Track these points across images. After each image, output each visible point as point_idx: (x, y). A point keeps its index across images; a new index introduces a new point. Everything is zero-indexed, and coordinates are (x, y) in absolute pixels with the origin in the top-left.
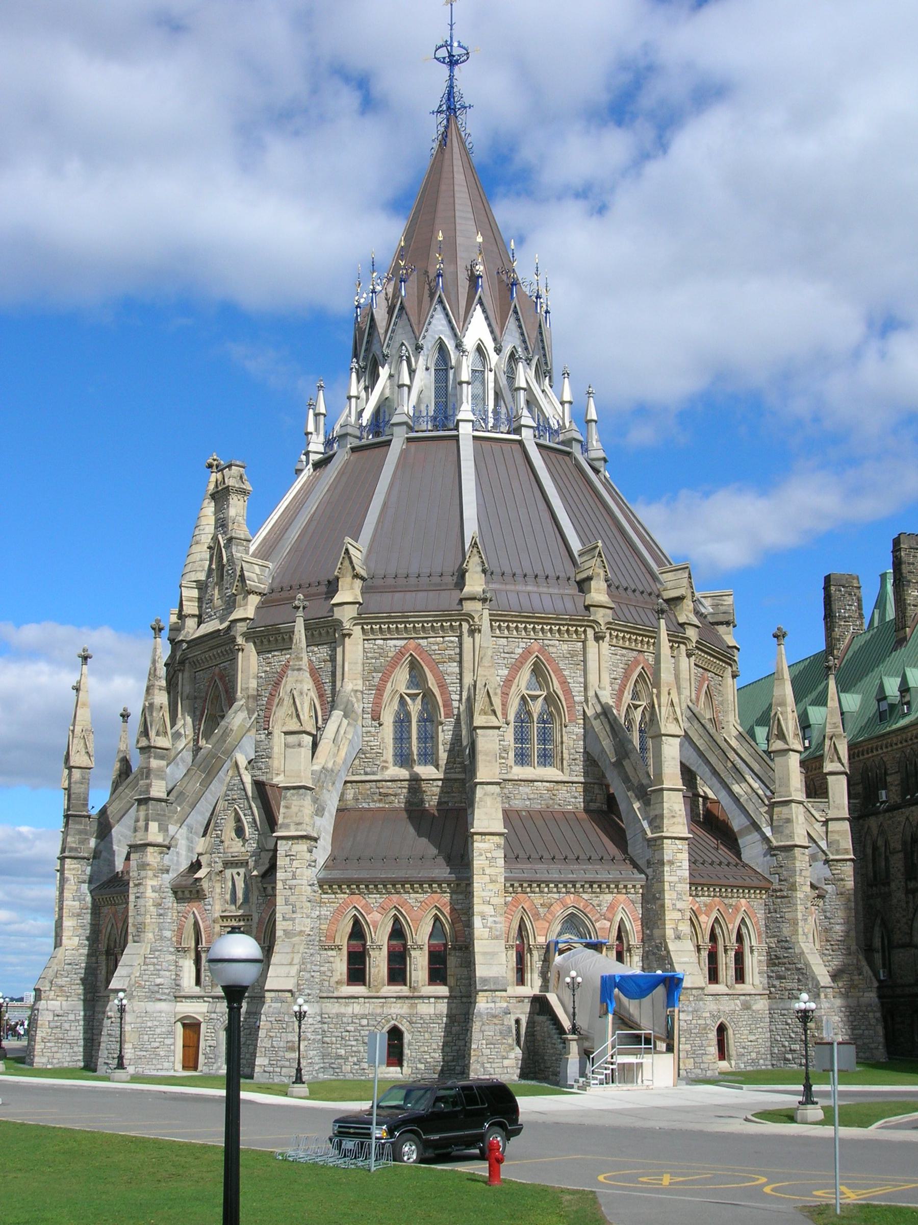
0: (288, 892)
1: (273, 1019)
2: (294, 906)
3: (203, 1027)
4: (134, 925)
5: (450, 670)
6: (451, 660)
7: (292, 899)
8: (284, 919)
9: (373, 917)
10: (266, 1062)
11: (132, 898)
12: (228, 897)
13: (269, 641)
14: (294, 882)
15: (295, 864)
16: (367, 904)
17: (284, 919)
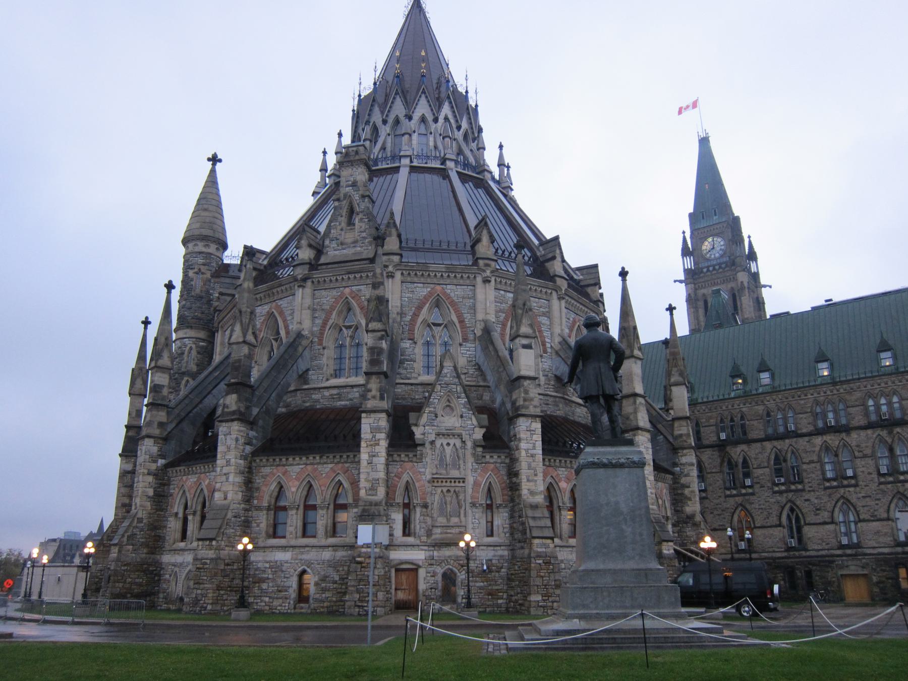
0: (530, 460)
1: (541, 562)
2: (535, 470)
3: (422, 573)
4: (367, 480)
5: (543, 322)
6: (544, 314)
7: (533, 464)
8: (528, 480)
9: (563, 485)
10: (539, 598)
11: (364, 456)
12: (436, 462)
13: (416, 274)
14: (534, 452)
15: (535, 437)
16: (558, 475)
17: (528, 480)
